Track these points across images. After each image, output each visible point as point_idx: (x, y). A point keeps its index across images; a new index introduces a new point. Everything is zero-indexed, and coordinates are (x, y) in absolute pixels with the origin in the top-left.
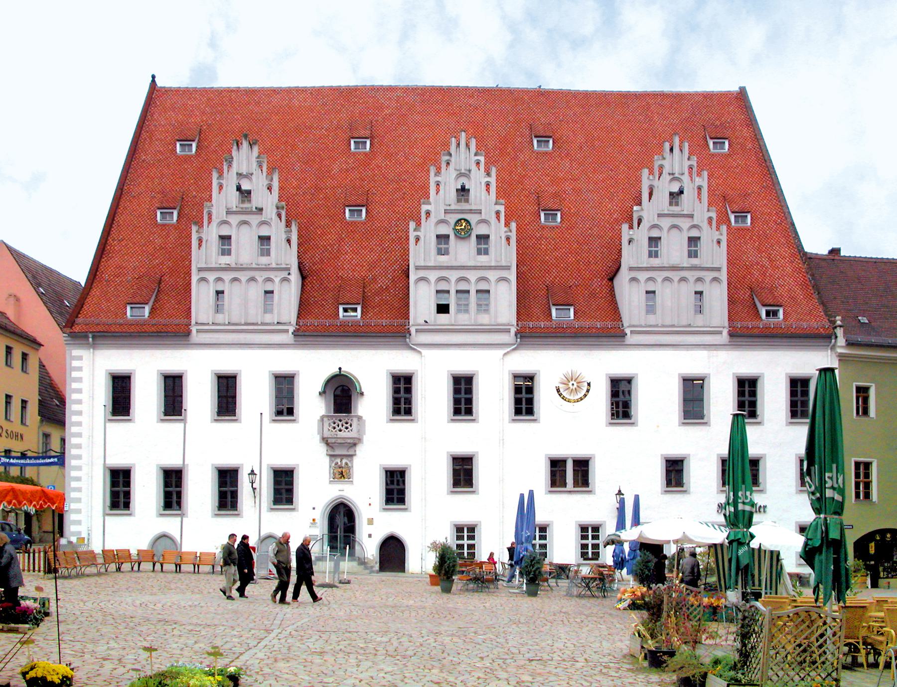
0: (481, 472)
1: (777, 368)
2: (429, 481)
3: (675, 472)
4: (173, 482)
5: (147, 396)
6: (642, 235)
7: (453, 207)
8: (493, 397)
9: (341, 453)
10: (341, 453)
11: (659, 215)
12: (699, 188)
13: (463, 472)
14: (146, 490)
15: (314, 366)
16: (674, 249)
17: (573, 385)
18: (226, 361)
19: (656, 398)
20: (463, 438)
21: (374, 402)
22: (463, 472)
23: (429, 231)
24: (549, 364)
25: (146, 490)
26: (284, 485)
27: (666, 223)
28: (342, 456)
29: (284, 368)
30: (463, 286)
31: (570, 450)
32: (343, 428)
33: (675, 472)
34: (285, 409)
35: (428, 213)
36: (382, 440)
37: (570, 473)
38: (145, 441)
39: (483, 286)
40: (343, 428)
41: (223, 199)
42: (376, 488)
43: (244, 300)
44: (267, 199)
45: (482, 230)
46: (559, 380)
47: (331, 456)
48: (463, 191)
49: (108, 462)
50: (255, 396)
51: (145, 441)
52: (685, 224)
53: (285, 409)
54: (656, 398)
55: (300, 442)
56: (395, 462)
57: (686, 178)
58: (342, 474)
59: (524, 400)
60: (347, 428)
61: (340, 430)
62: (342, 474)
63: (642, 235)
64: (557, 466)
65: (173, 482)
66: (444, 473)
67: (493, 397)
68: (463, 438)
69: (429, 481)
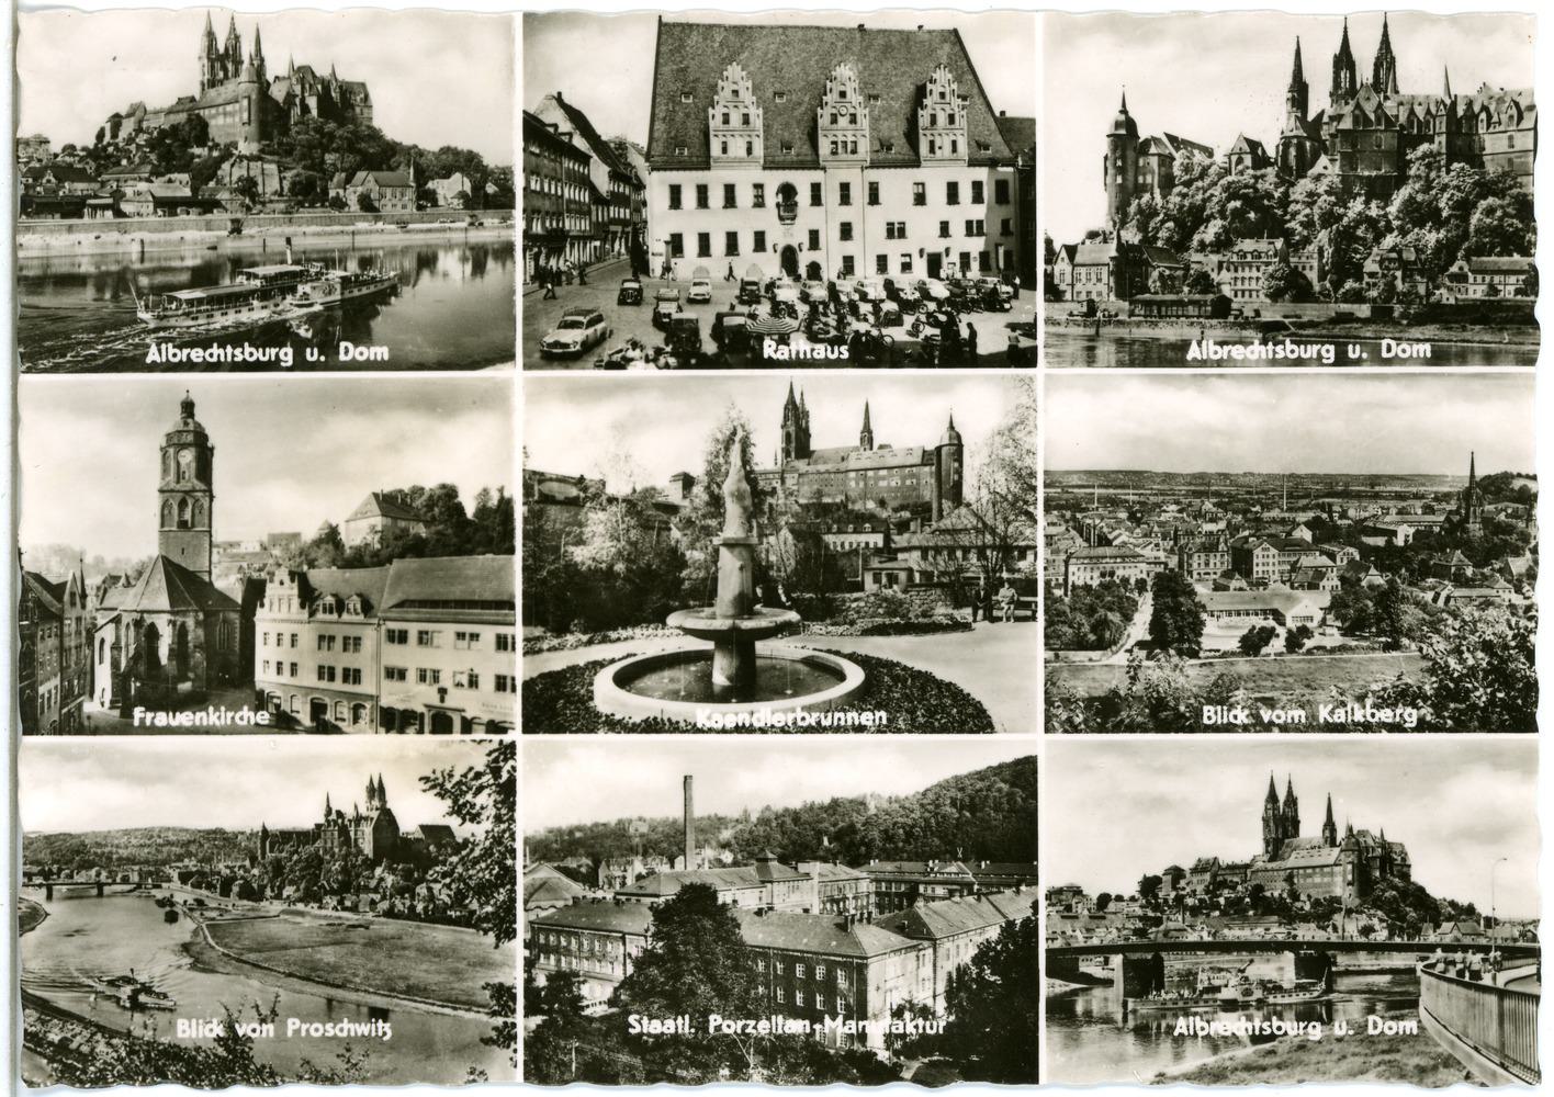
0: (856, 232)
2: (830, 235)
3: (945, 230)
5: (689, 197)
8: (859, 194)
13: (846, 231)
15: (773, 180)
18: (729, 176)
20: (846, 214)
21: (803, 197)
22: (846, 231)
24: (883, 177)
26: (760, 242)
27: (938, 107)
29: (758, 181)
31: (896, 219)
33: (945, 230)
34: (759, 203)
36: (808, 217)
37: (896, 231)
38: (689, 221)
41: (724, 96)
43: (737, 148)
44: (747, 97)
45: (852, 111)
50: (745, 196)
51: (689, 221)
52: (947, 107)
53: (759, 203)
54: (936, 194)
55: (768, 219)
59: (874, 198)
64: (890, 225)
66: (836, 232)
67: (859, 194)
68: (846, 214)
69: (830, 235)
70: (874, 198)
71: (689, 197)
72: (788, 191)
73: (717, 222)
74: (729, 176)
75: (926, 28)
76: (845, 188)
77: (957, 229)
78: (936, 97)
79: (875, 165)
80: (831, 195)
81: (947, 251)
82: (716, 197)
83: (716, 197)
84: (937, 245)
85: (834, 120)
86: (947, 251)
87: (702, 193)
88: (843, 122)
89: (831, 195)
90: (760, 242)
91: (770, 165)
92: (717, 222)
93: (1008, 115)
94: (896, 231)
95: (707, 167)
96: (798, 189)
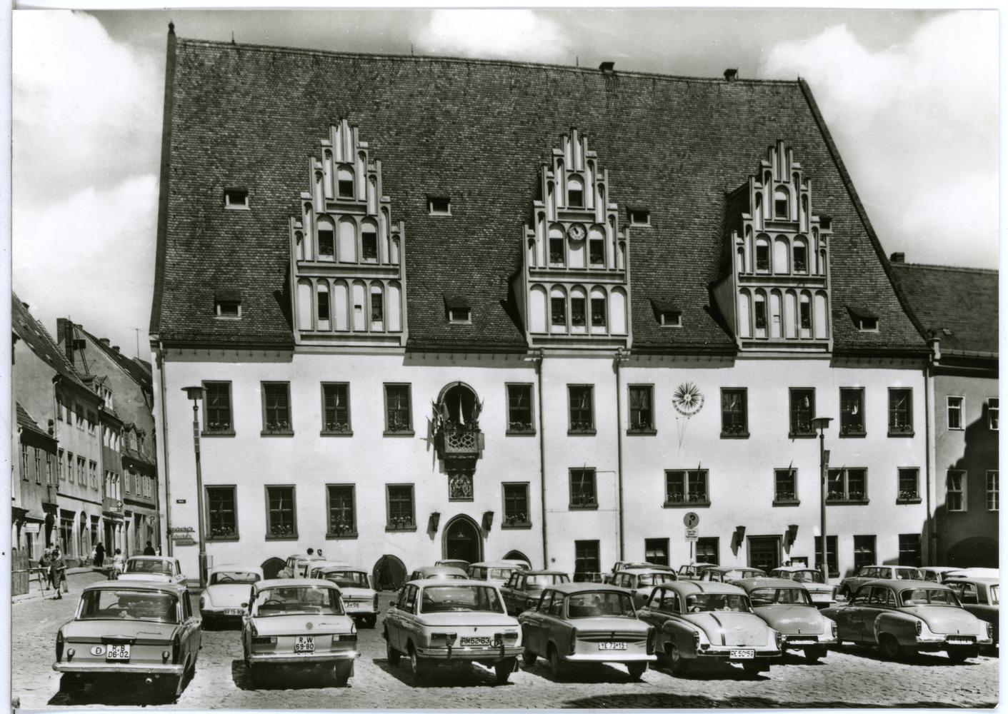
0: (605, 488)
1: (877, 384)
3: (786, 484)
4: (281, 504)
5: (247, 408)
6: (750, 244)
7: (565, 211)
8: (609, 408)
9: (460, 469)
10: (460, 469)
11: (768, 224)
12: (805, 197)
13: (583, 488)
14: (252, 513)
16: (781, 260)
17: (688, 397)
19: (771, 412)
20: (583, 452)
22: (583, 488)
23: (543, 235)
25: (252, 513)
26: (401, 502)
28: (460, 473)
30: (578, 294)
31: (687, 463)
32: (464, 443)
33: (786, 484)
35: (542, 216)
36: (501, 457)
38: (247, 459)
39: (598, 295)
40: (464, 443)
42: (497, 503)
43: (349, 303)
45: (595, 235)
46: (673, 393)
47: (451, 475)
48: (576, 197)
49: (205, 481)
50: (367, 408)
51: (247, 459)
54: (771, 412)
55: (412, 458)
56: (515, 477)
57: (791, 187)
58: (461, 493)
59: (642, 417)
60: (468, 443)
61: (462, 445)
62: (461, 493)
63: (750, 244)
64: (674, 478)
65: (281, 504)
67: (609, 408)
68: (583, 452)
70: (642, 421)
71: (247, 408)
72: (459, 402)
73: (308, 460)
74: (335, 367)
75: (742, 75)
76: (581, 397)
77: (809, 486)
78: (767, 211)
79: (648, 348)
80: (554, 409)
81: (792, 532)
82: (307, 408)
83: (307, 408)
84: (772, 521)
85: (557, 249)
86: (792, 532)
87: (277, 401)
88: (576, 259)
89: (554, 409)
91: (422, 346)
92: (308, 460)
93: (909, 260)
94: (687, 488)
95: (282, 346)
96: (482, 395)
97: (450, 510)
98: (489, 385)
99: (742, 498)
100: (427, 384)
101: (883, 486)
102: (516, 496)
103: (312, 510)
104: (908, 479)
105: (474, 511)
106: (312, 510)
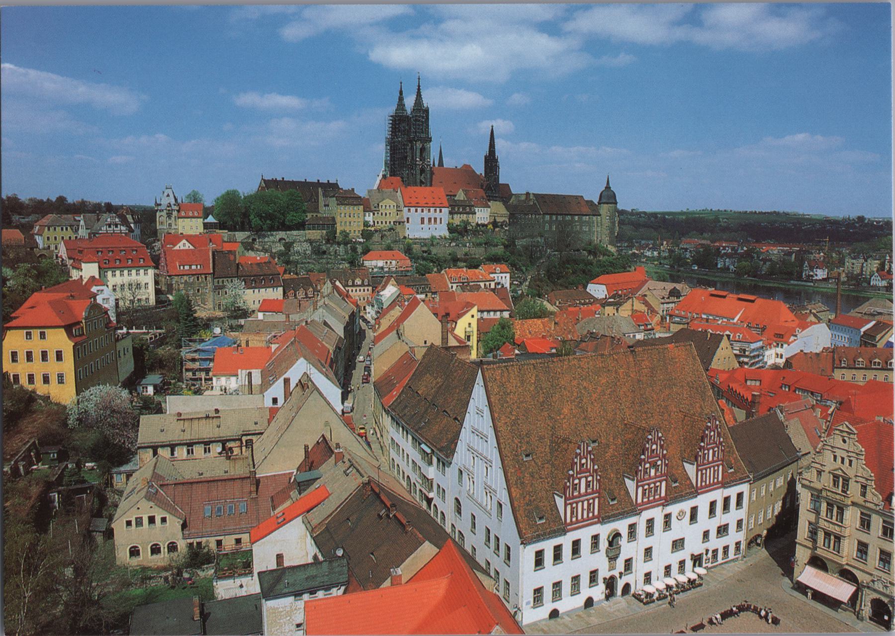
9: (612, 559)
10: (612, 559)
19: (703, 512)
54: (703, 512)
62: (612, 568)
73: (564, 571)
80: (641, 529)
89: (641, 529)
90: (593, 576)
97: (608, 576)
98: (622, 526)
99: (694, 546)
100: (604, 531)
101: (732, 528)
102: (628, 563)
103: (566, 588)
104: (739, 523)
105: (616, 573)
106: (566, 588)
